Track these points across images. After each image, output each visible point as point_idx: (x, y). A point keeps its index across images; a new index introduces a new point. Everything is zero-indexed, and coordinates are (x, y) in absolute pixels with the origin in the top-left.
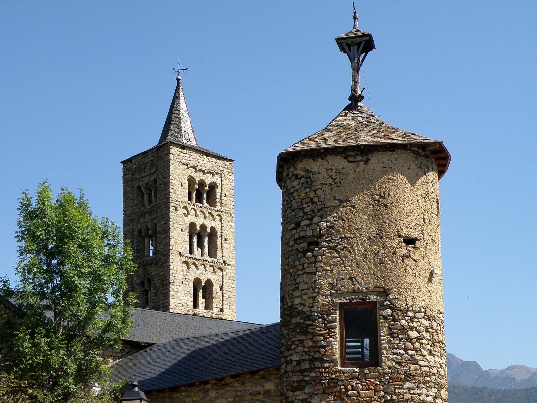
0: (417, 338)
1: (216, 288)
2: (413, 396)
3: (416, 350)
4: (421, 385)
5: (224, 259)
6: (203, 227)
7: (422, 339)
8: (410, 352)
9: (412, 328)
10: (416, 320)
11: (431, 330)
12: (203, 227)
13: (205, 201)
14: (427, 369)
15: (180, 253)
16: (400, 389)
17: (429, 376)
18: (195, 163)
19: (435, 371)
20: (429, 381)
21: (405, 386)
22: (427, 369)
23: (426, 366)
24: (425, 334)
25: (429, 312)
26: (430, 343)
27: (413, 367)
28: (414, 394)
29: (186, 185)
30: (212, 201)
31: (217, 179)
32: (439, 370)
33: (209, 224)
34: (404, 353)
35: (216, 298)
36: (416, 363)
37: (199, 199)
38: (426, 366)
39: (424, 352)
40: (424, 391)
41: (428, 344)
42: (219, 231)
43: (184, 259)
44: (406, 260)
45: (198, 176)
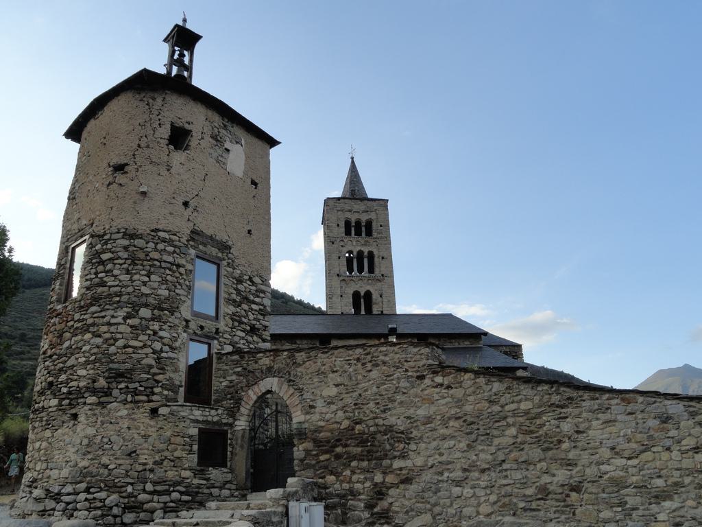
0: (110, 259)
1: (375, 296)
2: (96, 319)
3: (106, 272)
4: (107, 307)
5: (382, 273)
6: (360, 253)
7: (117, 259)
8: (100, 275)
9: (104, 252)
10: (112, 241)
11: (131, 249)
12: (360, 253)
13: (364, 234)
14: (118, 289)
15: (338, 275)
16: (85, 314)
17: (120, 296)
18: (349, 208)
19: (130, 289)
20: (119, 302)
21: (89, 311)
22: (118, 289)
23: (117, 286)
24: (120, 254)
25: (131, 232)
26: (129, 262)
27: (100, 289)
28: (97, 317)
29: (342, 224)
30: (369, 233)
31: (373, 216)
32: (136, 288)
33: (366, 250)
34: (104, 279)
35: (376, 303)
36: (102, 284)
37: (358, 233)
38: (117, 286)
39: (116, 272)
40: (111, 312)
41: (125, 263)
42: (376, 253)
43: (342, 278)
44: (111, 186)
45: (353, 218)
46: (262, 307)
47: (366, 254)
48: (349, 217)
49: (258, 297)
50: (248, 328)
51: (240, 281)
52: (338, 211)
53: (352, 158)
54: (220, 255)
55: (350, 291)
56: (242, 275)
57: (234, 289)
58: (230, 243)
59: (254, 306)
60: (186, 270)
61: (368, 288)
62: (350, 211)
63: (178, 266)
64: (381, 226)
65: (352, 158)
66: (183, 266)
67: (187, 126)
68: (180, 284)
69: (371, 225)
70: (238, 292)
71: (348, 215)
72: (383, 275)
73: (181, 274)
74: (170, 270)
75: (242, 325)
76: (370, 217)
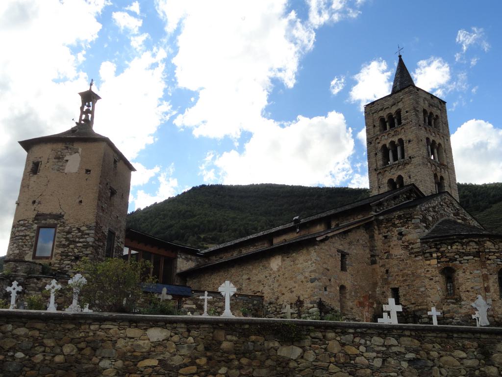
5: (409, 155)
6: (392, 143)
12: (392, 143)
29: (377, 123)
33: (396, 139)
37: (392, 125)
46: (86, 244)
47: (396, 142)
48: (382, 115)
49: (82, 238)
50: (73, 258)
51: (69, 232)
52: (373, 113)
53: (400, 56)
54: (56, 222)
55: (386, 181)
56: (71, 228)
57: (64, 238)
58: (63, 213)
59: (79, 245)
60: (30, 237)
61: (399, 173)
62: (382, 110)
63: (26, 236)
64: (407, 112)
65: (400, 56)
66: (28, 235)
67: (40, 160)
68: (26, 245)
69: (400, 114)
70: (67, 239)
71: (381, 114)
72: (410, 158)
73: (27, 240)
74: (21, 239)
75: (68, 257)
76: (398, 108)
